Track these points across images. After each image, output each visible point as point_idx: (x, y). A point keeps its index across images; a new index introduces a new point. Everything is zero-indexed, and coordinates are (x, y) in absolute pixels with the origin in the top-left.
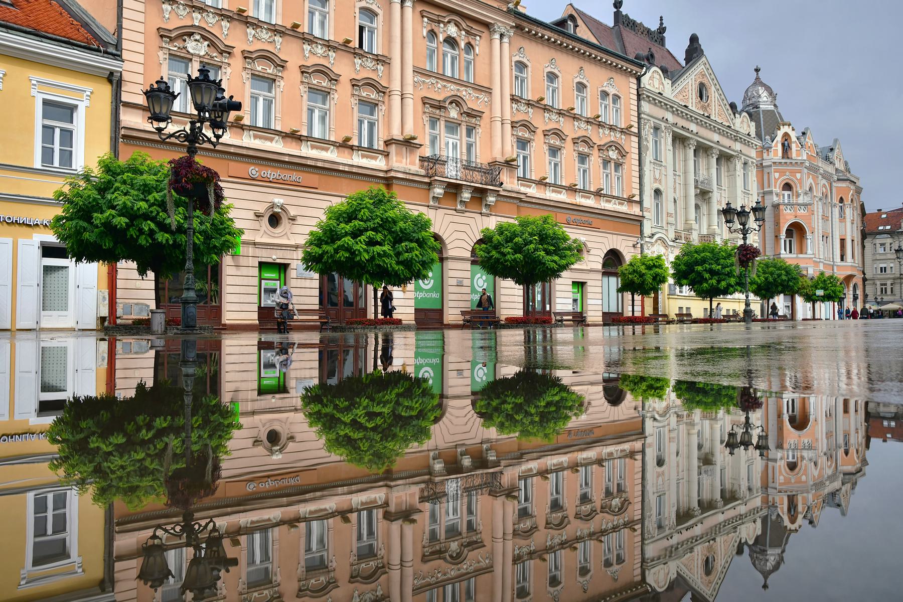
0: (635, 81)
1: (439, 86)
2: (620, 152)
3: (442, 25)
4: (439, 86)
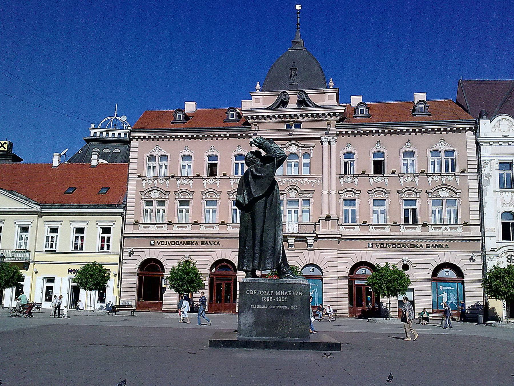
4: (284, 182)
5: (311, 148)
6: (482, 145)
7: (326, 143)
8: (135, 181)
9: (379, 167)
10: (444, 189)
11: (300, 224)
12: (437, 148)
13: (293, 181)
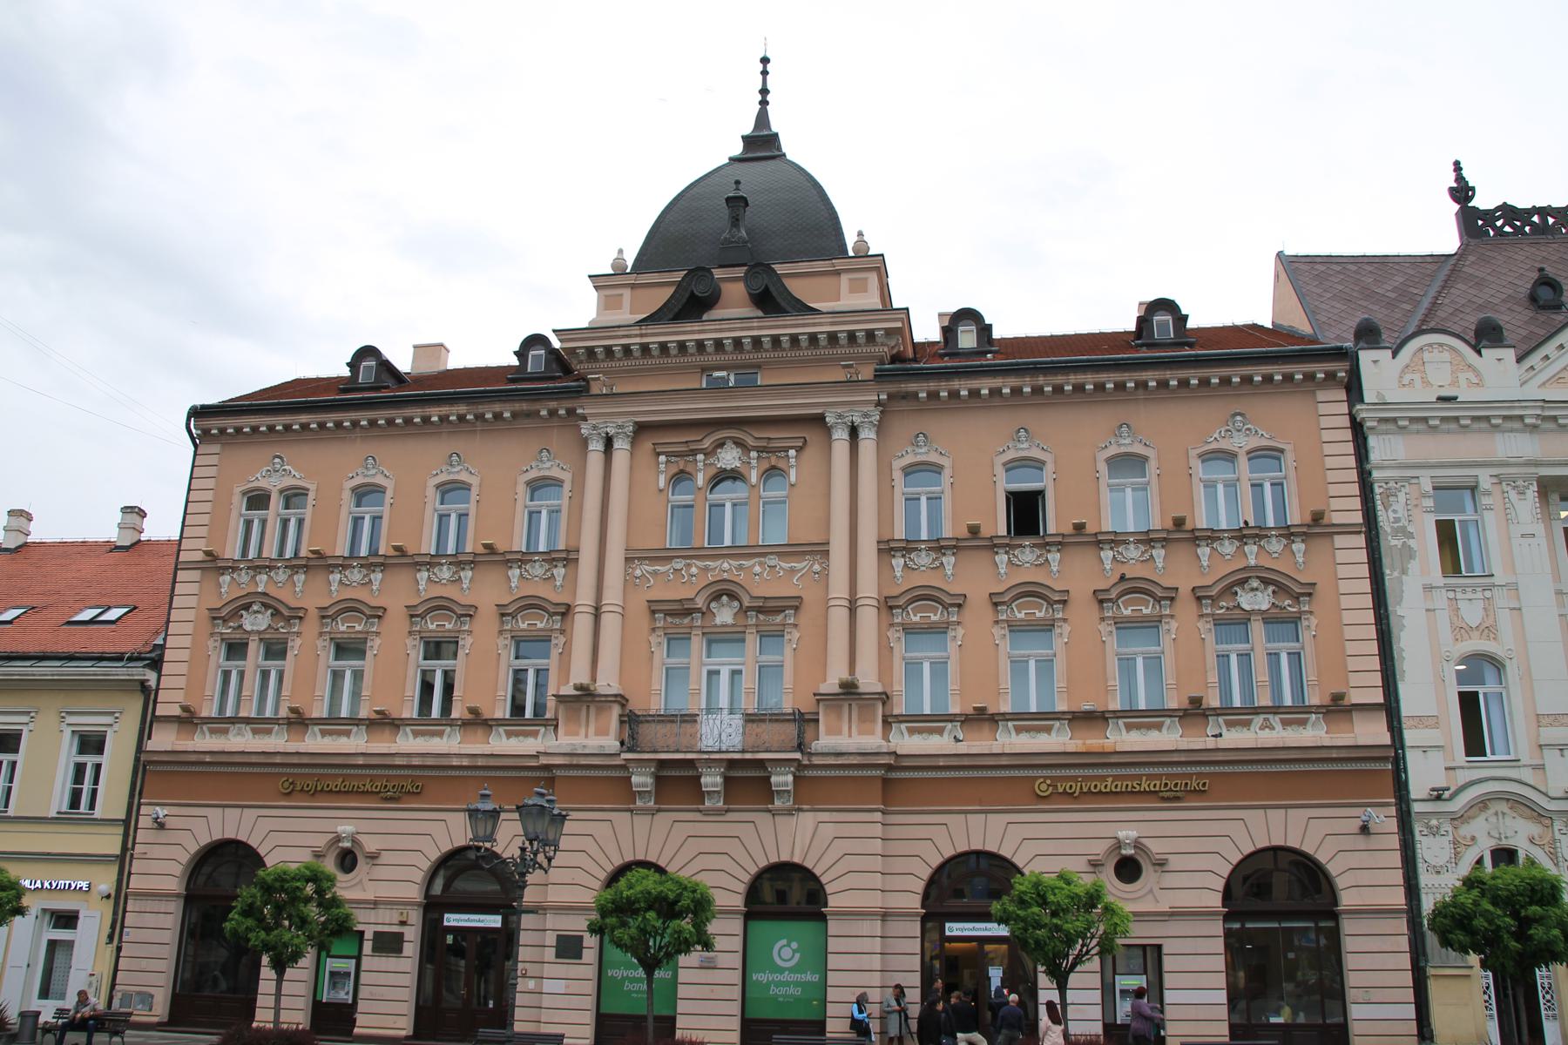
0: (1342, 395)
1: (694, 570)
2: (1281, 589)
3: (700, 457)
4: (694, 570)
5: (792, 453)
6: (1372, 428)
7: (841, 435)
8: (195, 575)
9: (1025, 512)
10: (1255, 583)
11: (750, 719)
12: (1224, 444)
13: (726, 565)
